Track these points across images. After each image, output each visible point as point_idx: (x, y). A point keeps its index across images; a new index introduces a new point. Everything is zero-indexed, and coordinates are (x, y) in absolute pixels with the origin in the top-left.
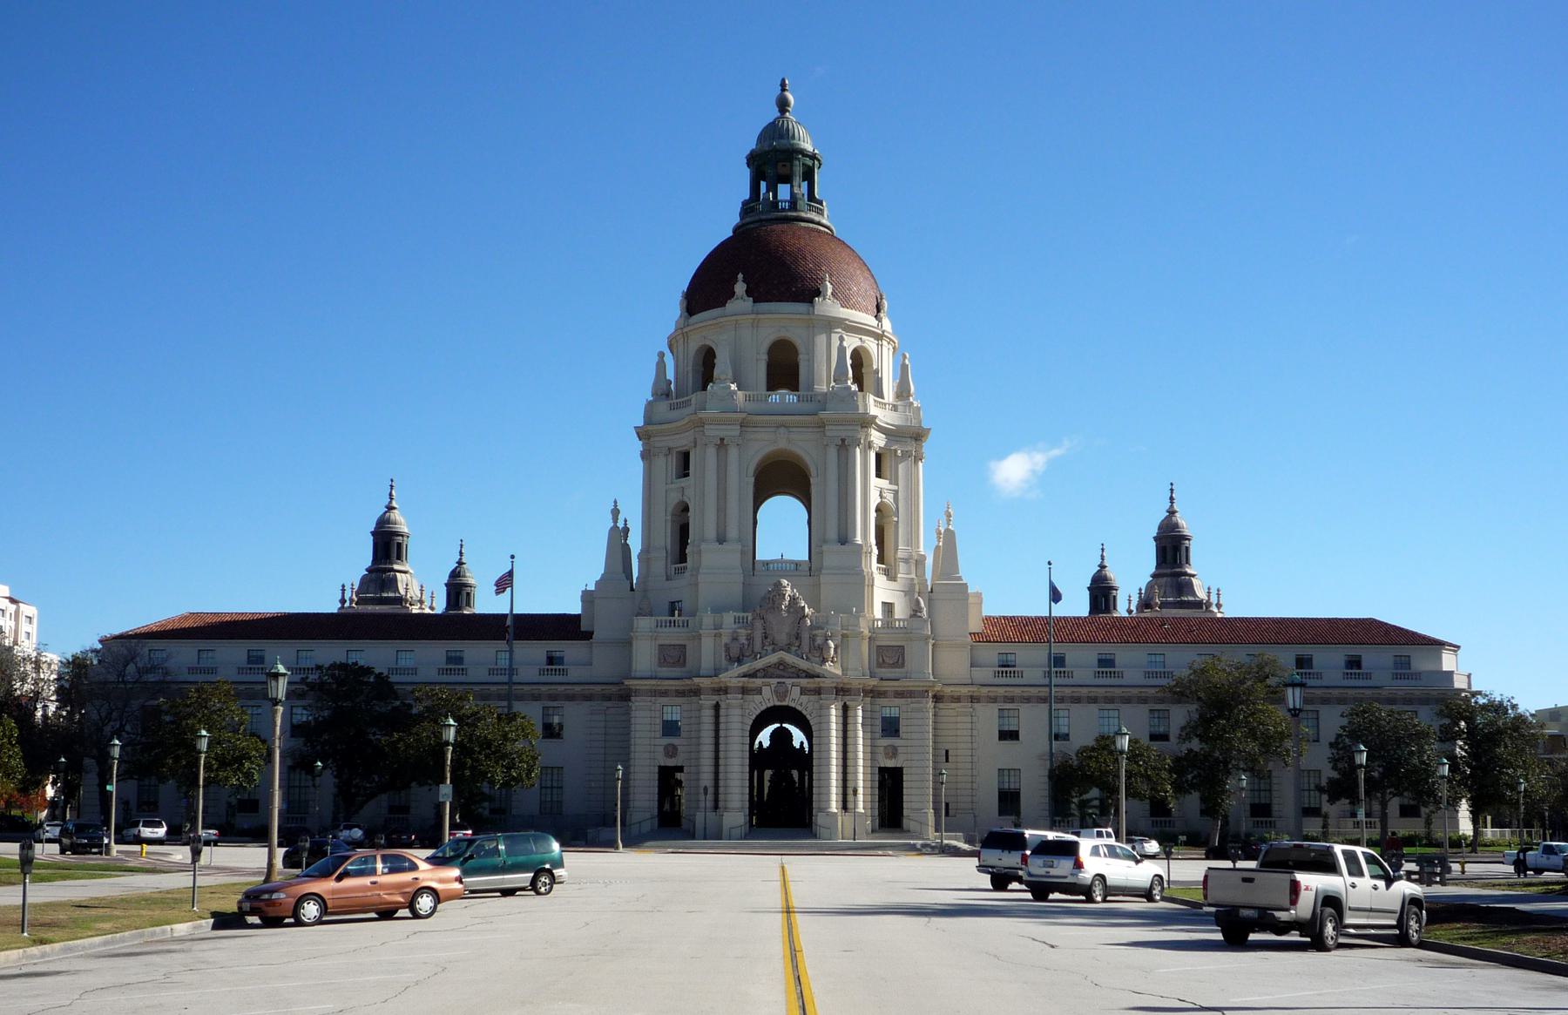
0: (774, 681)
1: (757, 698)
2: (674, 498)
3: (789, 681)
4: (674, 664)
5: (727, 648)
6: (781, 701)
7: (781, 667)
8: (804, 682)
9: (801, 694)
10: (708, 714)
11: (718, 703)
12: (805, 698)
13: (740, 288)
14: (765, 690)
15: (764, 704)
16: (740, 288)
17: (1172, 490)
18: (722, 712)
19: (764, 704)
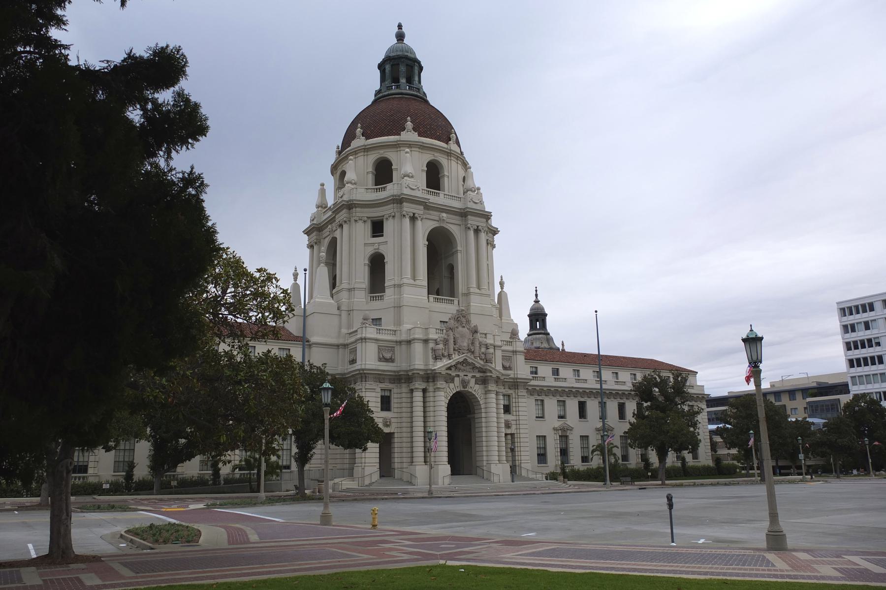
0: (461, 374)
1: (452, 385)
2: (370, 251)
3: (470, 375)
4: (387, 360)
5: (434, 350)
6: (464, 388)
7: (464, 365)
8: (478, 375)
9: (475, 384)
10: (418, 396)
11: (426, 387)
12: (477, 387)
13: (409, 125)
14: (456, 379)
15: (454, 389)
16: (409, 125)
17: (536, 291)
18: (428, 394)
19: (454, 389)
